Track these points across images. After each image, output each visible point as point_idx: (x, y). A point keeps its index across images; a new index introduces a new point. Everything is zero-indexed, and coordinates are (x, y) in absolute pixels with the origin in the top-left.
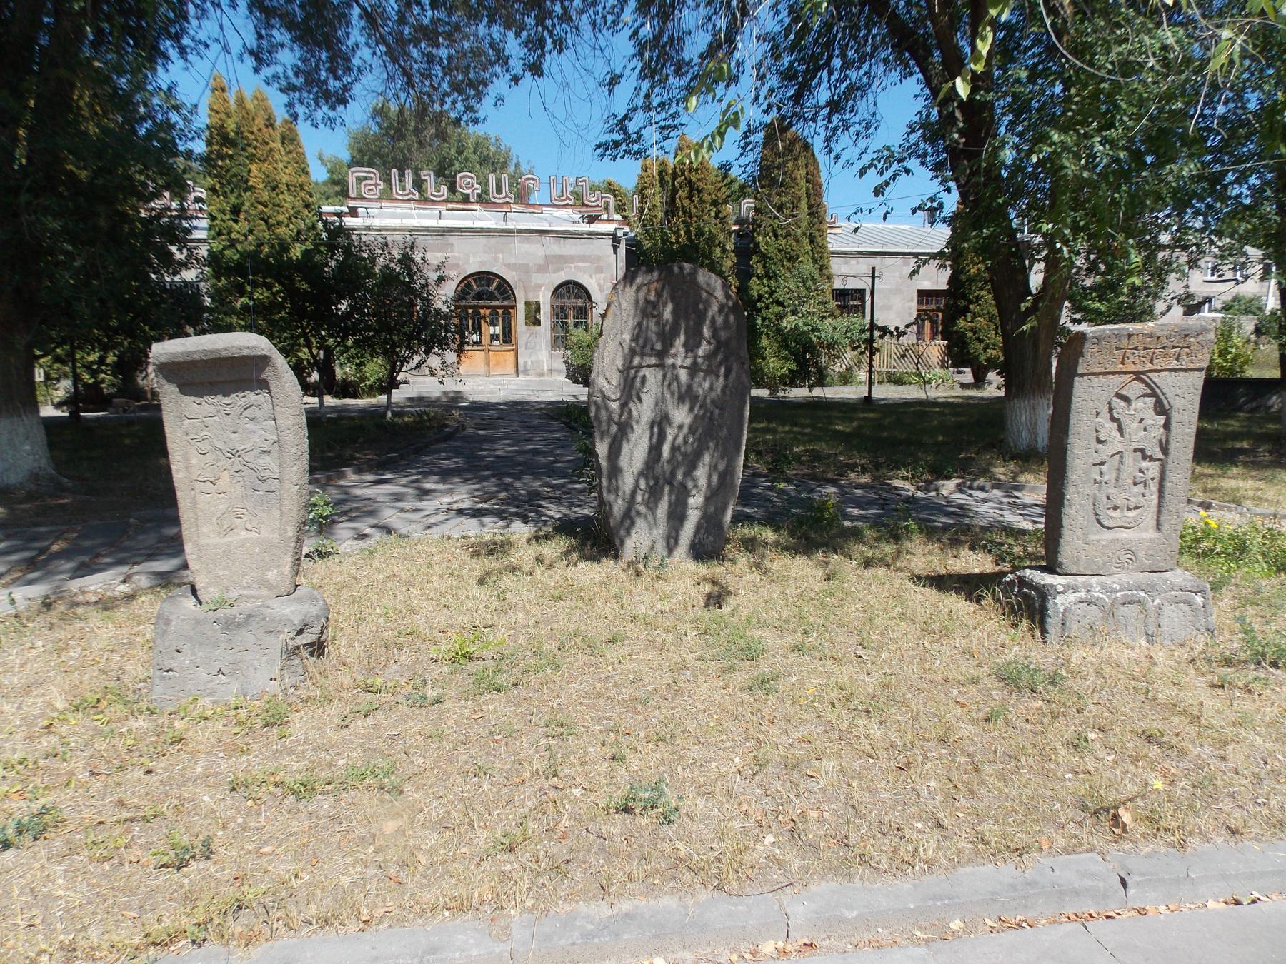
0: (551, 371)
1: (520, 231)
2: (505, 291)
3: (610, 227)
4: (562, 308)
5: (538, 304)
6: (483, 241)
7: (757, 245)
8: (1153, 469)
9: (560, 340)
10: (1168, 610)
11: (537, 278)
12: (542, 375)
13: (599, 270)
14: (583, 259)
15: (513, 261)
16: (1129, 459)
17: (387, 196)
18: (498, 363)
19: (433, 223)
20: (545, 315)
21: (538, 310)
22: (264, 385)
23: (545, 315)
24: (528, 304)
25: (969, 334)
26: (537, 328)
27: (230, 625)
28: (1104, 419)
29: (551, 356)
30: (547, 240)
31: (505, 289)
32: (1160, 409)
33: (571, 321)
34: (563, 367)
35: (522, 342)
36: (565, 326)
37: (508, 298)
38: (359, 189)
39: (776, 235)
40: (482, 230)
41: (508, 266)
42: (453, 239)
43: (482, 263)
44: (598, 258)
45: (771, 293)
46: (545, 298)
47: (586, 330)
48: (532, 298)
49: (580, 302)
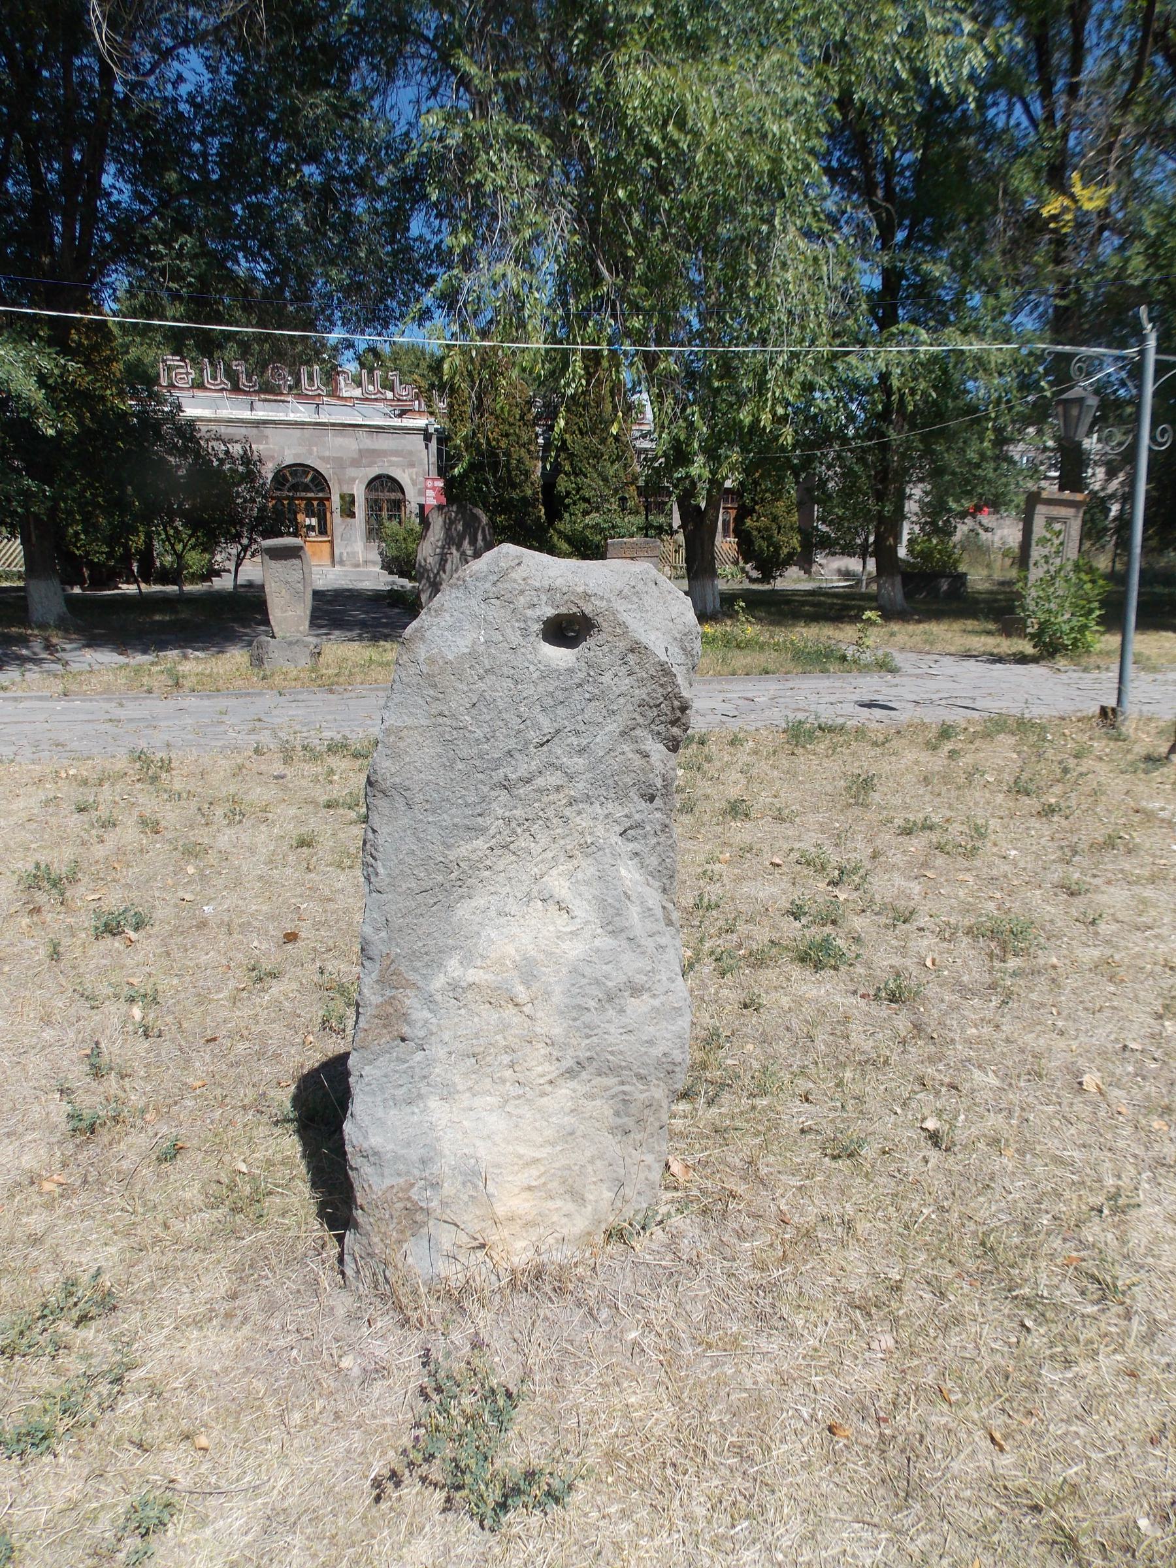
0: (366, 562)
1: (333, 425)
2: (320, 484)
3: (421, 422)
4: (376, 501)
6: (296, 433)
9: (374, 532)
11: (351, 472)
12: (358, 566)
13: (412, 465)
14: (396, 453)
15: (327, 454)
18: (314, 554)
19: (246, 414)
20: (360, 508)
21: (353, 502)
23: (360, 508)
24: (342, 497)
25: (755, 533)
26: (349, 520)
27: (290, 644)
29: (366, 547)
30: (361, 434)
31: (320, 481)
33: (384, 514)
34: (379, 559)
35: (338, 531)
37: (322, 490)
38: (170, 378)
39: (581, 433)
40: (296, 423)
41: (322, 458)
42: (268, 431)
43: (296, 455)
44: (410, 453)
45: (578, 490)
46: (359, 492)
47: (400, 523)
48: (346, 490)
49: (393, 496)
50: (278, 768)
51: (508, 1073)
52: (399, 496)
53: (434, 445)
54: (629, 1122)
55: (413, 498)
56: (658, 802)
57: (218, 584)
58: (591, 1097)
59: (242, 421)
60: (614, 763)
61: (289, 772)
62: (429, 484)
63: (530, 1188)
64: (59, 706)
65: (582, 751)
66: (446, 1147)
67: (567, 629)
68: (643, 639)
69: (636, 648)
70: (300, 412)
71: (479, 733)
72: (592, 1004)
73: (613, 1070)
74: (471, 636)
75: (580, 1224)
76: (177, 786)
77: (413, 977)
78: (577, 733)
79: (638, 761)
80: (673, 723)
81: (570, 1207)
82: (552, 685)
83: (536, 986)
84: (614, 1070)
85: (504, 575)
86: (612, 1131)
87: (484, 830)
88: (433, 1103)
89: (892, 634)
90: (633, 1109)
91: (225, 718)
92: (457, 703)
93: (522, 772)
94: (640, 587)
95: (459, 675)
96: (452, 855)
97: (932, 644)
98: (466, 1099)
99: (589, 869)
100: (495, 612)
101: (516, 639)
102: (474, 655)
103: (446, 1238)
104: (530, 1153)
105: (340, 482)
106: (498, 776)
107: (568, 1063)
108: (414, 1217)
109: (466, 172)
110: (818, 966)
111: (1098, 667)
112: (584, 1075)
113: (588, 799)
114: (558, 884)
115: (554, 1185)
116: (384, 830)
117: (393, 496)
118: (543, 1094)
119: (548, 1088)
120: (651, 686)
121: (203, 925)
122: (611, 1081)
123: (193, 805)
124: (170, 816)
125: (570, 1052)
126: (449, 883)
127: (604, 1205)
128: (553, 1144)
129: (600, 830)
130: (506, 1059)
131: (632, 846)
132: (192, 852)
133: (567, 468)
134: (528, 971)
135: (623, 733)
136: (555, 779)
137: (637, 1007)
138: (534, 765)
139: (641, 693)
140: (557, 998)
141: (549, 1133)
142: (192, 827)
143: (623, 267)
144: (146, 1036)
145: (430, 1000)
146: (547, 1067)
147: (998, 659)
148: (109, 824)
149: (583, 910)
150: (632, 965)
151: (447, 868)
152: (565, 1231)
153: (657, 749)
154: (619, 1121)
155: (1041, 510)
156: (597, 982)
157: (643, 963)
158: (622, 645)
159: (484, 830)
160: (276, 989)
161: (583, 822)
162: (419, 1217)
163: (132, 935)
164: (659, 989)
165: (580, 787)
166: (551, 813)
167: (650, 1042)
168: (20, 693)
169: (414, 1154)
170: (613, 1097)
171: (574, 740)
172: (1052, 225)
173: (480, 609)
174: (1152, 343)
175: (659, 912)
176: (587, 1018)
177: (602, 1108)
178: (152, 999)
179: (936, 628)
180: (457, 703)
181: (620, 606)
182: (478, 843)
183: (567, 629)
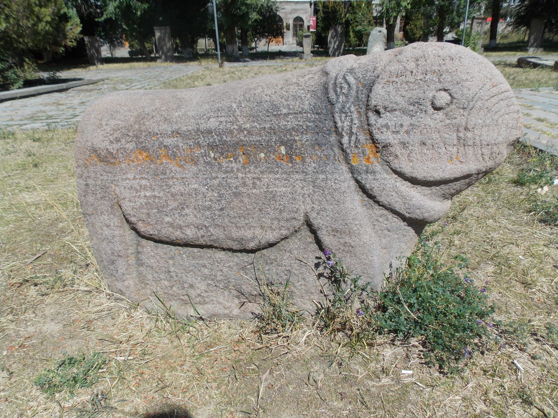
0: (293, 44)
9: (295, 34)
11: (289, 16)
13: (306, 13)
14: (302, 9)
30: (292, 4)
33: (298, 29)
34: (296, 42)
36: (296, 31)
44: (306, 9)
46: (291, 22)
52: (302, 23)
53: (313, 6)
55: (306, 24)
67: (380, 32)
105: (286, 19)
183: (380, 32)
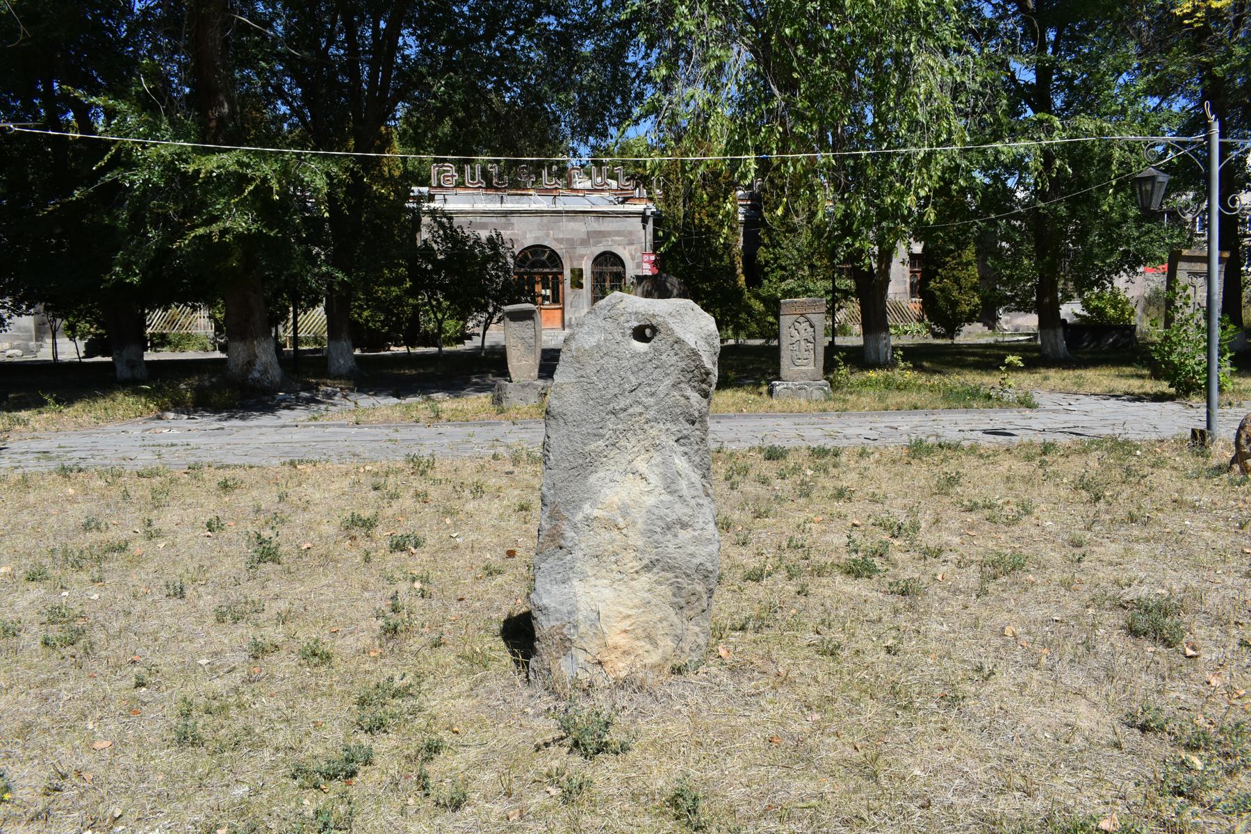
1: (567, 212)
2: (555, 261)
3: (640, 207)
4: (601, 273)
5: (581, 270)
7: (764, 219)
8: (811, 346)
10: (816, 392)
11: (581, 250)
14: (618, 233)
15: (561, 236)
16: (803, 343)
17: (460, 184)
18: (548, 319)
19: (497, 206)
20: (587, 280)
22: (533, 319)
23: (587, 280)
24: (572, 271)
25: (938, 293)
27: (523, 386)
28: (792, 329)
31: (555, 259)
32: (812, 326)
33: (607, 284)
35: (567, 302)
37: (556, 266)
38: (439, 180)
41: (557, 240)
42: (514, 219)
43: (537, 238)
44: (631, 233)
45: (776, 259)
46: (586, 266)
48: (576, 266)
49: (615, 269)
50: (510, 468)
51: (614, 567)
53: (650, 226)
54: (683, 602)
56: (697, 425)
57: (469, 345)
58: (660, 583)
59: (494, 212)
60: (670, 401)
61: (516, 471)
62: (646, 258)
63: (626, 631)
64: (354, 431)
65: (652, 395)
66: (581, 605)
68: (682, 337)
69: (678, 341)
70: (543, 203)
71: (600, 386)
72: (658, 530)
73: (671, 569)
74: (597, 337)
75: (654, 658)
76: (438, 476)
77: (566, 514)
78: (649, 385)
79: (683, 401)
80: (703, 381)
81: (649, 647)
82: (637, 360)
83: (629, 518)
84: (671, 569)
85: (613, 306)
86: (672, 605)
87: (602, 436)
88: (575, 582)
89: (1046, 378)
90: (684, 593)
91: (472, 439)
92: (590, 370)
93: (622, 405)
94: (682, 311)
95: (591, 356)
96: (587, 449)
97: (1080, 386)
98: (592, 581)
99: (658, 458)
100: (609, 325)
101: (619, 338)
102: (598, 346)
103: (581, 657)
104: (626, 612)
105: (571, 259)
106: (610, 407)
107: (646, 561)
108: (565, 644)
109: (667, 22)
110: (858, 576)
111: (1230, 404)
112: (655, 570)
113: (656, 420)
114: (641, 465)
115: (639, 631)
116: (553, 436)
117: (615, 269)
118: (633, 579)
119: (636, 576)
120: (687, 361)
121: (456, 547)
122: (670, 575)
123: (450, 488)
124: (434, 493)
125: (647, 555)
126: (585, 464)
127: (670, 651)
128: (638, 608)
129: (663, 438)
130: (613, 559)
131: (683, 448)
132: (449, 512)
133: (766, 241)
134: (624, 511)
135: (673, 386)
136: (639, 409)
137: (685, 535)
138: (628, 402)
139: (682, 364)
140: (640, 526)
141: (637, 601)
142: (448, 500)
143: (790, 86)
144: (423, 596)
145: (575, 527)
146: (634, 563)
147: (1138, 398)
148: (394, 496)
149: (654, 480)
150: (680, 511)
151: (583, 455)
152: (646, 661)
153: (695, 397)
154: (676, 600)
155: (1182, 266)
156: (661, 518)
157: (688, 511)
158: (671, 340)
159: (602, 436)
160: (499, 579)
161: (653, 432)
162: (567, 644)
163: (413, 550)
164: (698, 526)
165: (652, 413)
166: (637, 427)
167: (692, 555)
168: (325, 422)
169: (565, 609)
170: (671, 584)
171: (648, 389)
172: (1186, 22)
173: (600, 322)
174: (1216, 128)
175: (699, 486)
176: (656, 537)
177: (666, 590)
178: (425, 580)
179: (1090, 374)
180: (590, 370)
181: (670, 321)
182: (600, 443)
